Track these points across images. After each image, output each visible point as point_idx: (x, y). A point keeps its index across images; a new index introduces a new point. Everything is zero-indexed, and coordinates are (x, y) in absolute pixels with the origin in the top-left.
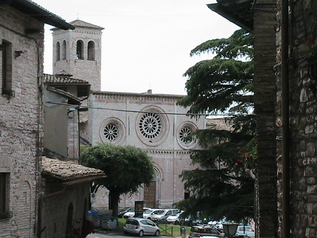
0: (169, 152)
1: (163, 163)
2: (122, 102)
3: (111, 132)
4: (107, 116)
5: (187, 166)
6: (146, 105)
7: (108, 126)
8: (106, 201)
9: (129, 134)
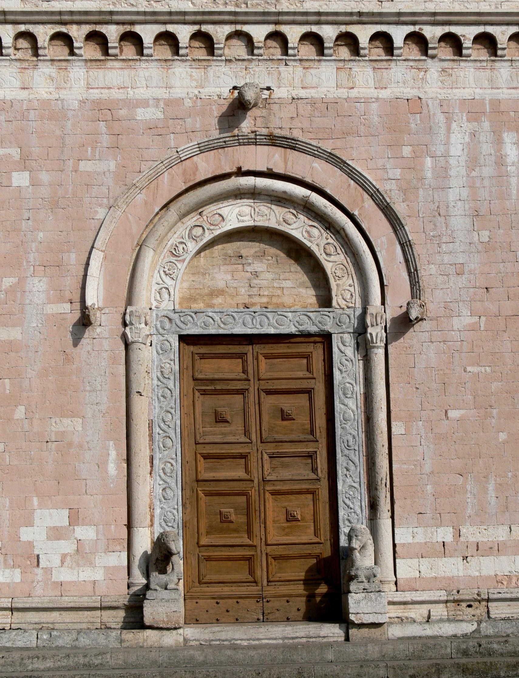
1: (407, 151)
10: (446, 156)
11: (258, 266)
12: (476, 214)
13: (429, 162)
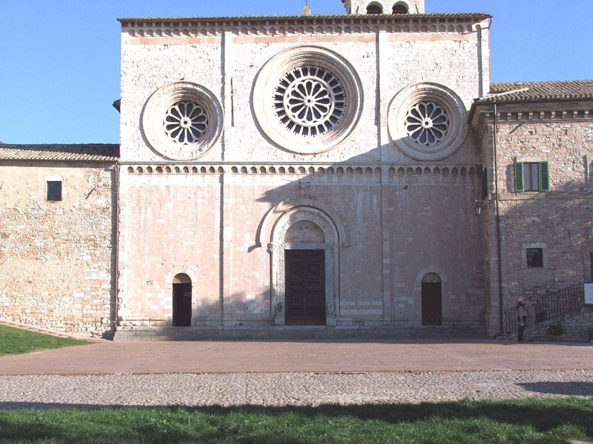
0: (364, 167)
2: (210, 41)
3: (186, 122)
4: (165, 79)
5: (429, 208)
6: (288, 45)
7: (177, 108)
8: (162, 303)
9: (233, 125)
10: (357, 201)
11: (305, 231)
12: (364, 218)
13: (352, 203)
